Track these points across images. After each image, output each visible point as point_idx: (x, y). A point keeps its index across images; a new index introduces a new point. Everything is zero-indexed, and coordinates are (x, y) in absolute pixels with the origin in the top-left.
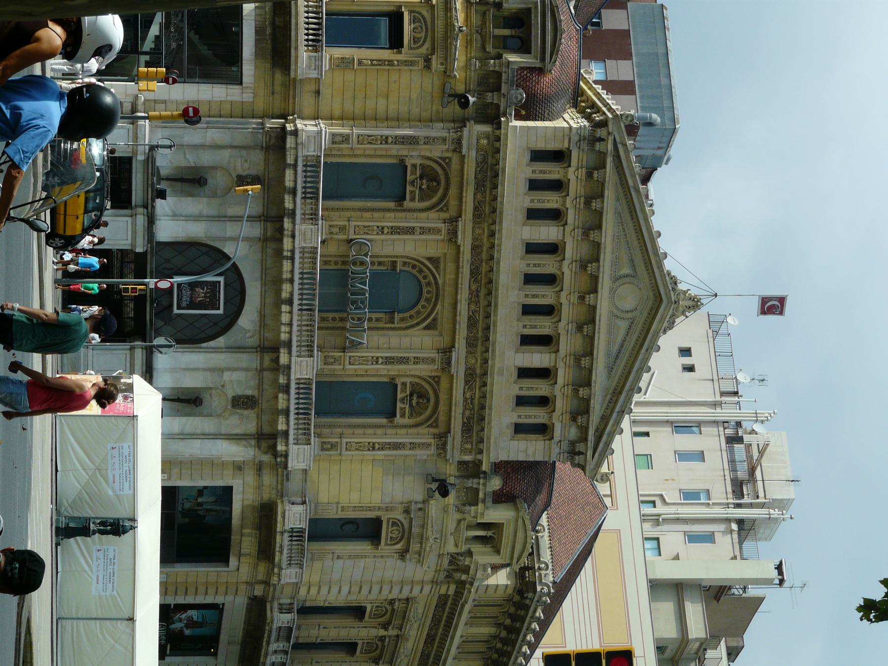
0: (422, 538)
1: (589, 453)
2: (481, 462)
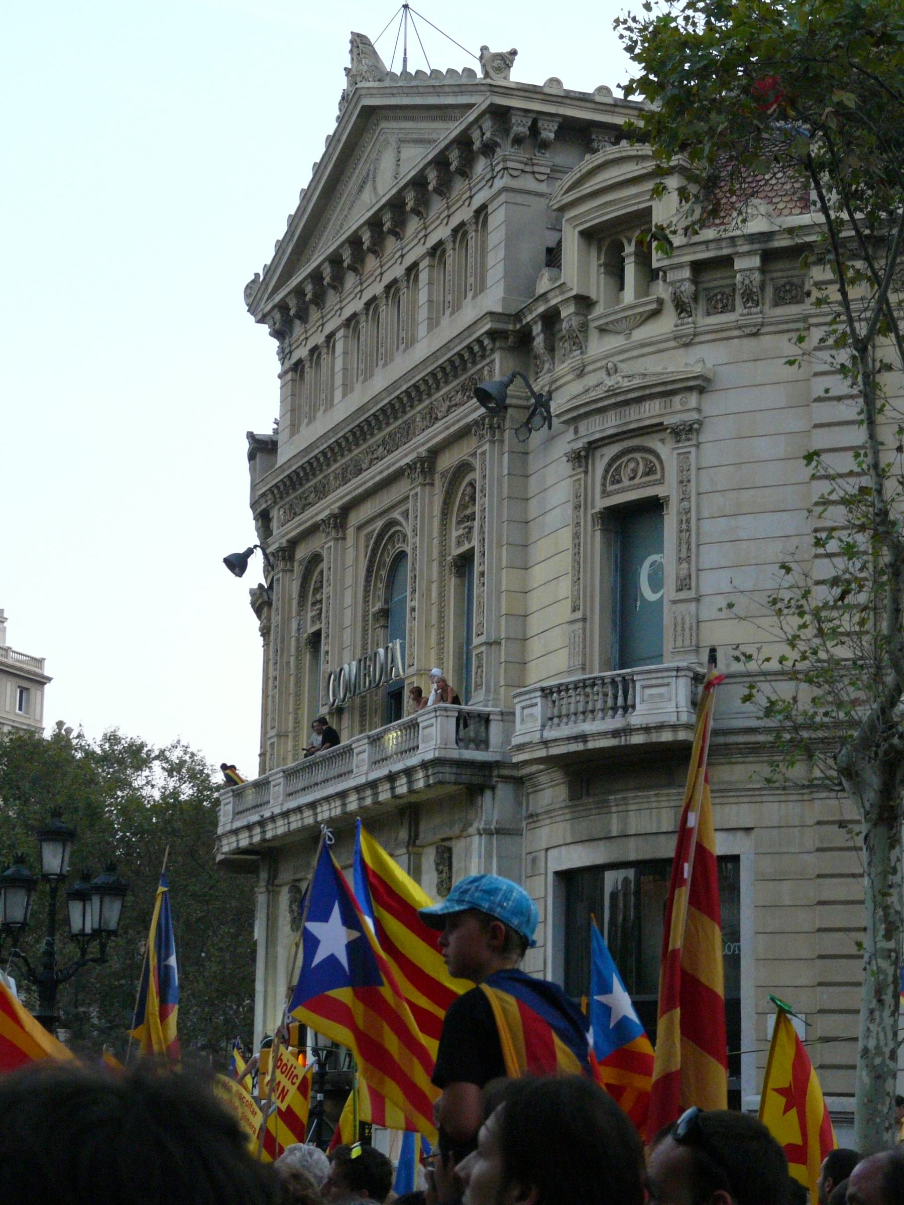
0: (627, 403)
1: (472, 116)
2: (493, 334)
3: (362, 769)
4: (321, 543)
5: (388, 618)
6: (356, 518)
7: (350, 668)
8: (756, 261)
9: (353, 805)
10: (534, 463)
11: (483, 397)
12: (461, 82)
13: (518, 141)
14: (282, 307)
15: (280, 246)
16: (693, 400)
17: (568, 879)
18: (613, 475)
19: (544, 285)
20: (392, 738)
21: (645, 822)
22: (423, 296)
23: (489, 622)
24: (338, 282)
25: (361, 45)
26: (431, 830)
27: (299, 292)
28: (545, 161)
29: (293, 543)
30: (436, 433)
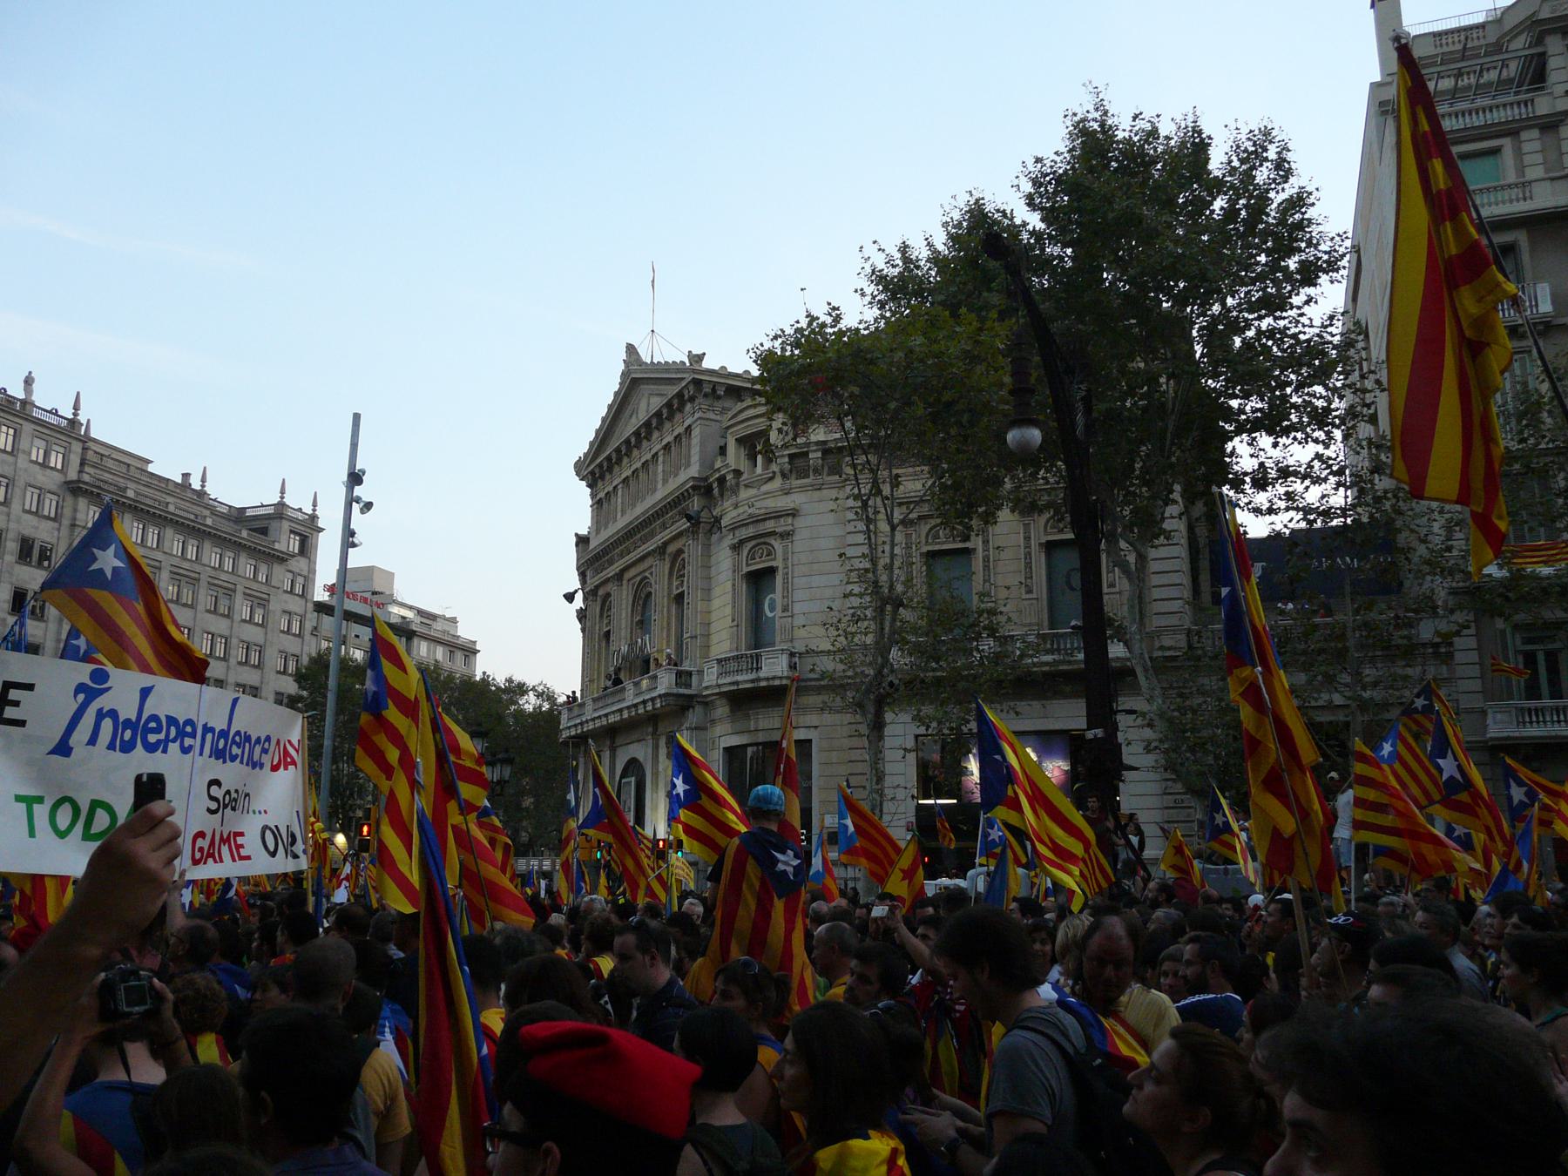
2: (693, 487)
3: (630, 697)
4: (611, 588)
5: (643, 624)
6: (627, 576)
7: (625, 649)
8: (819, 454)
9: (626, 715)
10: (714, 549)
11: (689, 518)
12: (678, 367)
13: (706, 396)
14: (592, 473)
15: (592, 444)
16: (790, 520)
17: (730, 751)
18: (751, 556)
19: (718, 464)
20: (645, 683)
21: (767, 723)
22: (660, 468)
23: (692, 626)
24: (619, 461)
25: (631, 349)
26: (663, 728)
27: (600, 465)
28: (719, 405)
29: (597, 587)
30: (666, 535)
